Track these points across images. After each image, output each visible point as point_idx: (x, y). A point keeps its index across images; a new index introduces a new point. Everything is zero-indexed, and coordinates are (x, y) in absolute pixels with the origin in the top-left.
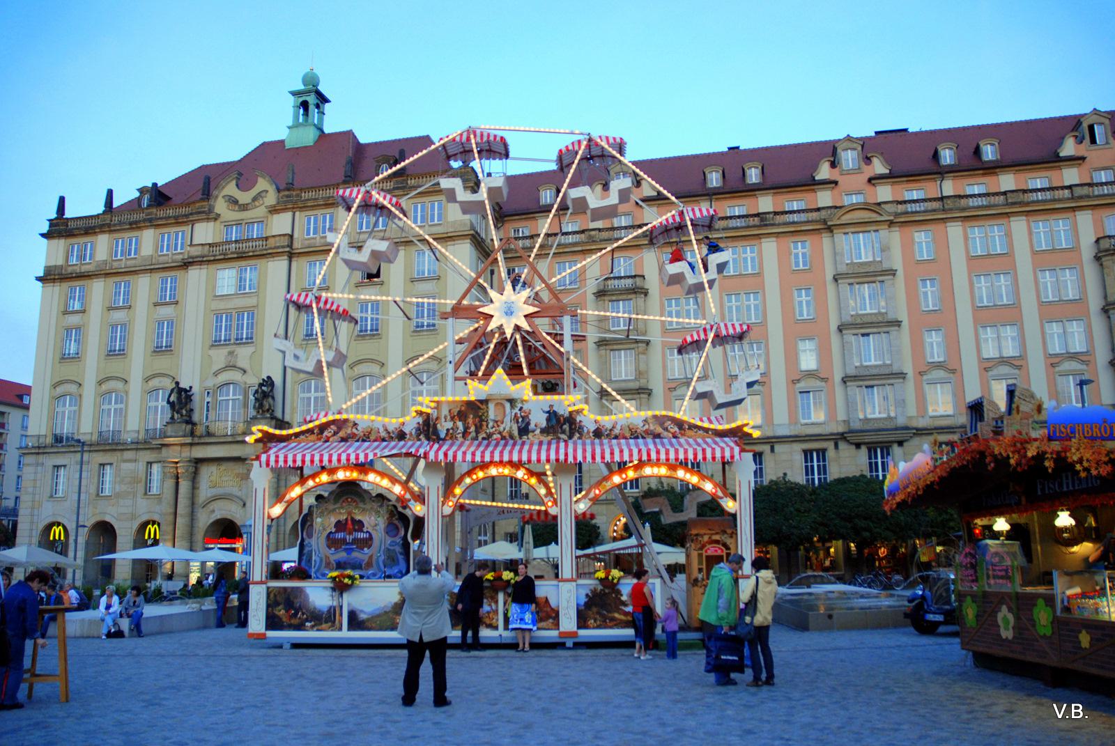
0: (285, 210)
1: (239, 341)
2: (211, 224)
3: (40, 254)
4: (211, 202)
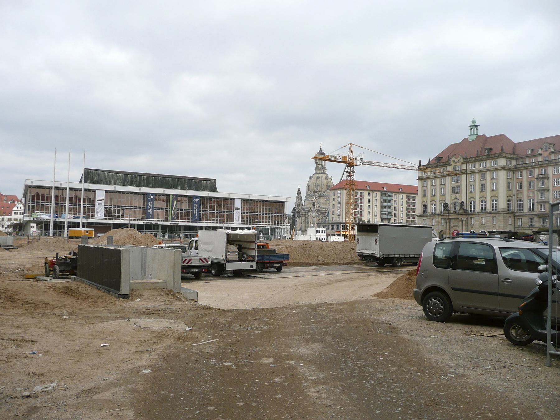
0: (464, 163)
1: (457, 193)
2: (450, 166)
3: (417, 174)
4: (450, 161)
